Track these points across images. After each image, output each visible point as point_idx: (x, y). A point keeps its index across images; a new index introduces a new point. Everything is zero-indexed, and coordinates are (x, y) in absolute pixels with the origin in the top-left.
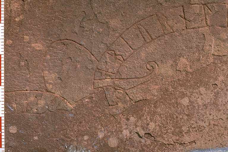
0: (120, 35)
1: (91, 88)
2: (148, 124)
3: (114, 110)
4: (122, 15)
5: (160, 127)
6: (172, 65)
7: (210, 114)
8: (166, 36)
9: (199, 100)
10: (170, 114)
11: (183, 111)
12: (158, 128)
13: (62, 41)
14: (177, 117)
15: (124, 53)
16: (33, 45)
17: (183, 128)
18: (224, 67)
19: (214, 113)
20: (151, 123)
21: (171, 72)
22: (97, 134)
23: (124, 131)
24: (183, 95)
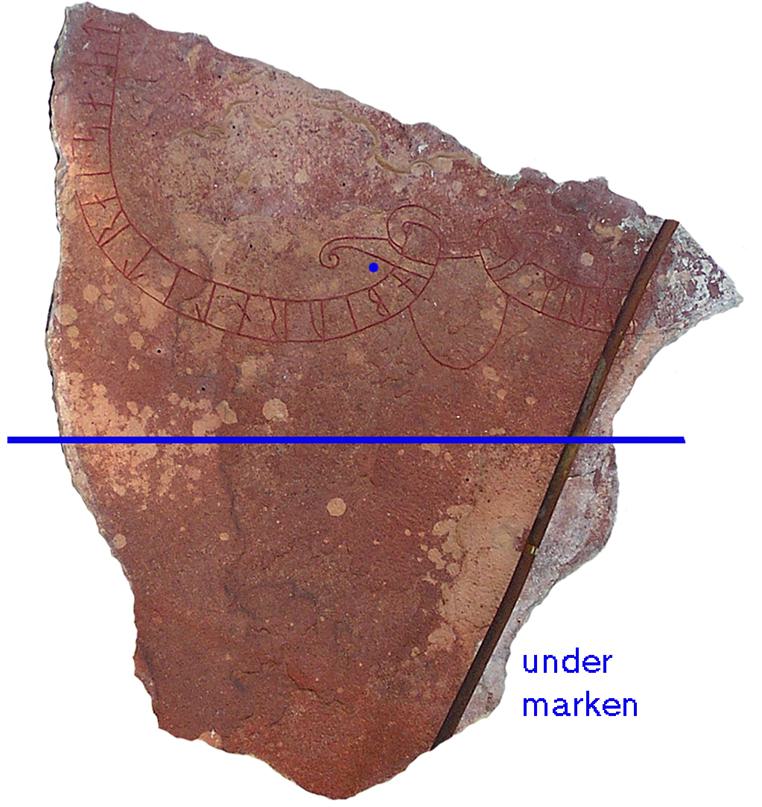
6: (298, 246)
8: (285, 297)
16: (497, 379)
18: (215, 204)
22: (463, 190)
23: (417, 175)
24: (298, 188)
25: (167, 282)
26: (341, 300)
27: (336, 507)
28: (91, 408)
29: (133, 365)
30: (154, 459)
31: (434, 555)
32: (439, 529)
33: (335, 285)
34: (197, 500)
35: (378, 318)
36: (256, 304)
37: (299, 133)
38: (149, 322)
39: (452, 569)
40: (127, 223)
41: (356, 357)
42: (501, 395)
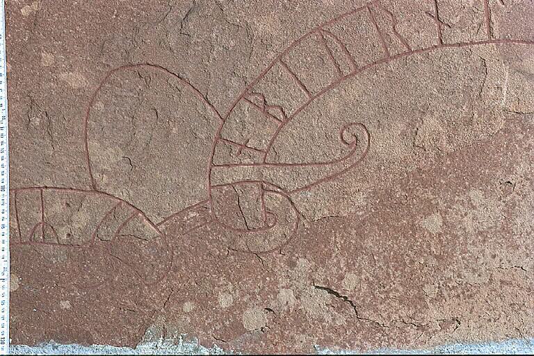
0: (280, 58)
1: (202, 185)
2: (341, 278)
3: (260, 241)
4: (284, 6)
5: (371, 284)
6: (403, 134)
7: (494, 257)
8: (391, 62)
9: (467, 221)
10: (395, 253)
11: (429, 246)
13: (136, 69)
14: (412, 262)
15: (288, 101)
16: (63, 76)
17: (427, 289)
19: (502, 253)
20: (348, 275)
21: (399, 151)
24: (430, 208)
26: (318, 89)
33: (333, 105)
35: (262, 87)
36: (426, 37)
37: (459, 276)
40: (220, 142)
42: (47, 59)
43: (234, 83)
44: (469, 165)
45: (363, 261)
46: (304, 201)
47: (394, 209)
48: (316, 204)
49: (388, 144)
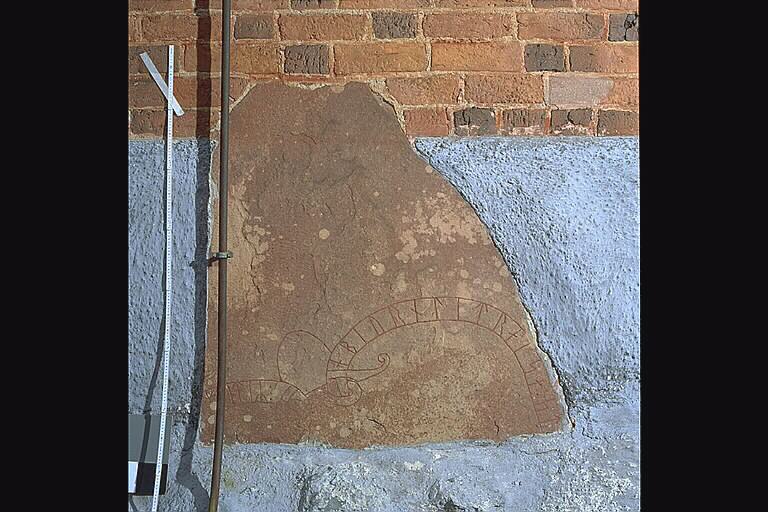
1: (324, 379)
9: (430, 393)
12: (389, 419)
19: (444, 405)
24: (414, 387)
25: (461, 310)
27: (324, 234)
28: (473, 230)
29: (461, 261)
30: (430, 218)
31: (262, 232)
32: (265, 246)
34: (399, 207)
38: (462, 286)
39: (248, 228)
41: (347, 315)
42: (262, 329)
43: (335, 338)
44: (427, 370)
45: (388, 409)
46: (364, 385)
47: (399, 388)
48: (368, 386)
49: (397, 362)
